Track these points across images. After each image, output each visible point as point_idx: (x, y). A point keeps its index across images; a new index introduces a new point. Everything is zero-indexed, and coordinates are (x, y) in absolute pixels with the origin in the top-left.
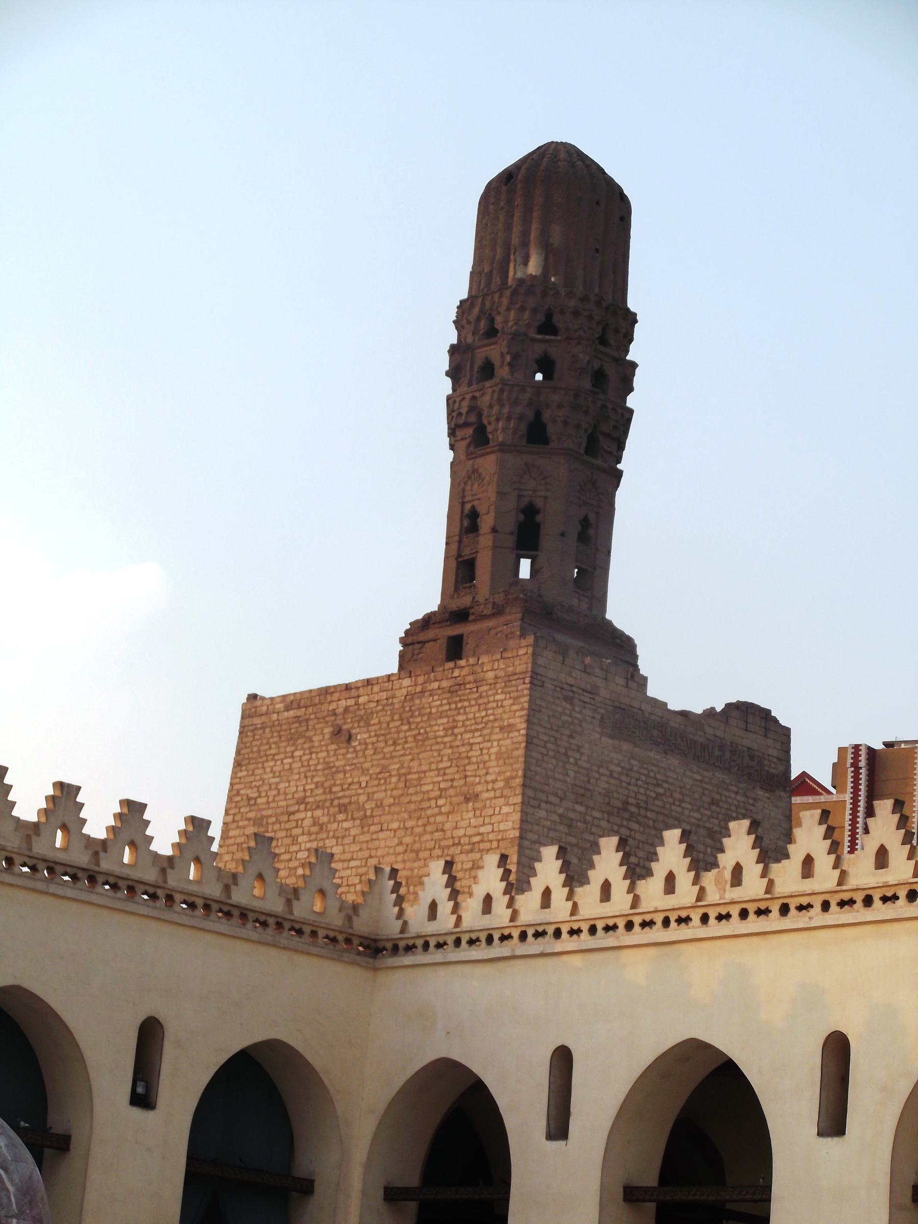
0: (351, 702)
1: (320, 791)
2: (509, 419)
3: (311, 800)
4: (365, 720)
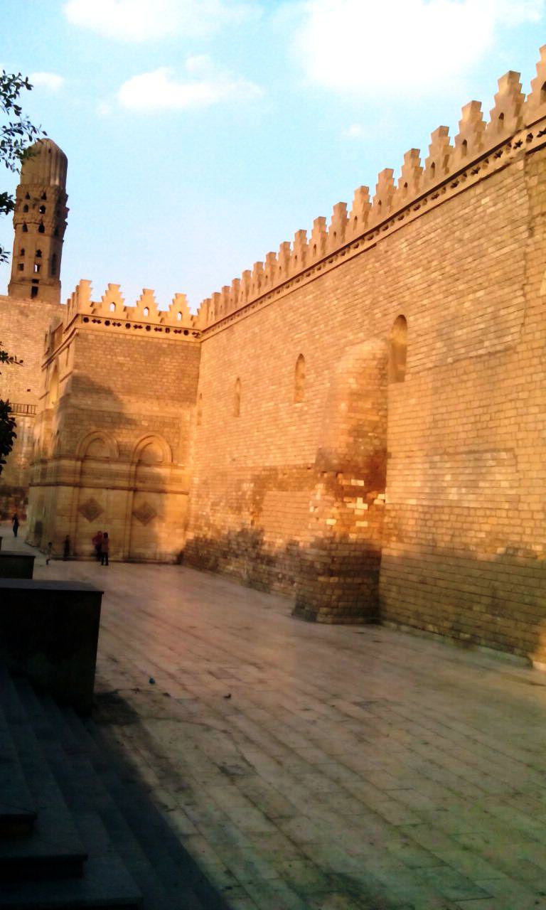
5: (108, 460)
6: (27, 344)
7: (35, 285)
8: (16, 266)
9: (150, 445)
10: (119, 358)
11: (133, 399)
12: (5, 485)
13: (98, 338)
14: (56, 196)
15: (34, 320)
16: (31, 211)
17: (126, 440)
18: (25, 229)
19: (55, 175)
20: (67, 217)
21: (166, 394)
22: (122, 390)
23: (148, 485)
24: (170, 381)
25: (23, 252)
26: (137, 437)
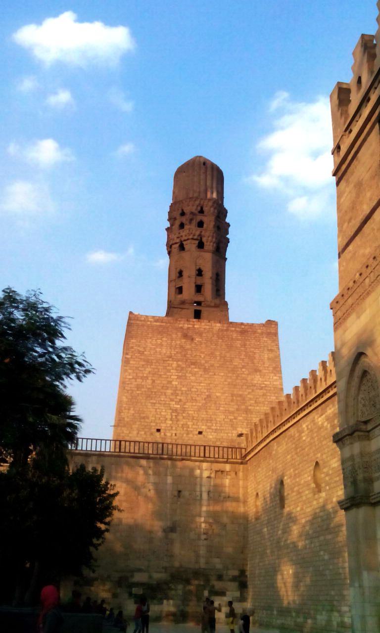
0: (189, 326)
1: (179, 355)
2: (214, 243)
3: (175, 357)
4: (200, 334)
6: (194, 374)
7: (198, 308)
8: (173, 289)
12: (181, 566)
14: (215, 208)
15: (201, 343)
16: (186, 227)
18: (182, 247)
19: (212, 188)
20: (228, 234)
25: (180, 274)
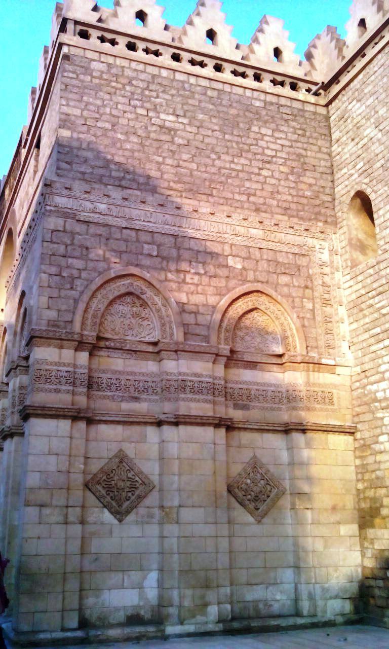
5: (156, 350)
9: (249, 316)
10: (163, 116)
11: (205, 209)
13: (114, 71)
17: (197, 299)
21: (275, 203)
22: (178, 186)
23: (255, 414)
24: (277, 175)
26: (222, 295)
